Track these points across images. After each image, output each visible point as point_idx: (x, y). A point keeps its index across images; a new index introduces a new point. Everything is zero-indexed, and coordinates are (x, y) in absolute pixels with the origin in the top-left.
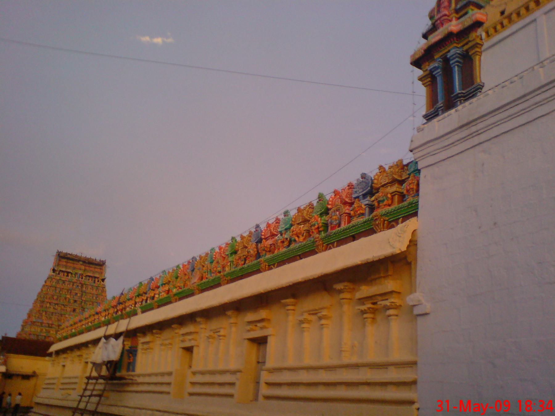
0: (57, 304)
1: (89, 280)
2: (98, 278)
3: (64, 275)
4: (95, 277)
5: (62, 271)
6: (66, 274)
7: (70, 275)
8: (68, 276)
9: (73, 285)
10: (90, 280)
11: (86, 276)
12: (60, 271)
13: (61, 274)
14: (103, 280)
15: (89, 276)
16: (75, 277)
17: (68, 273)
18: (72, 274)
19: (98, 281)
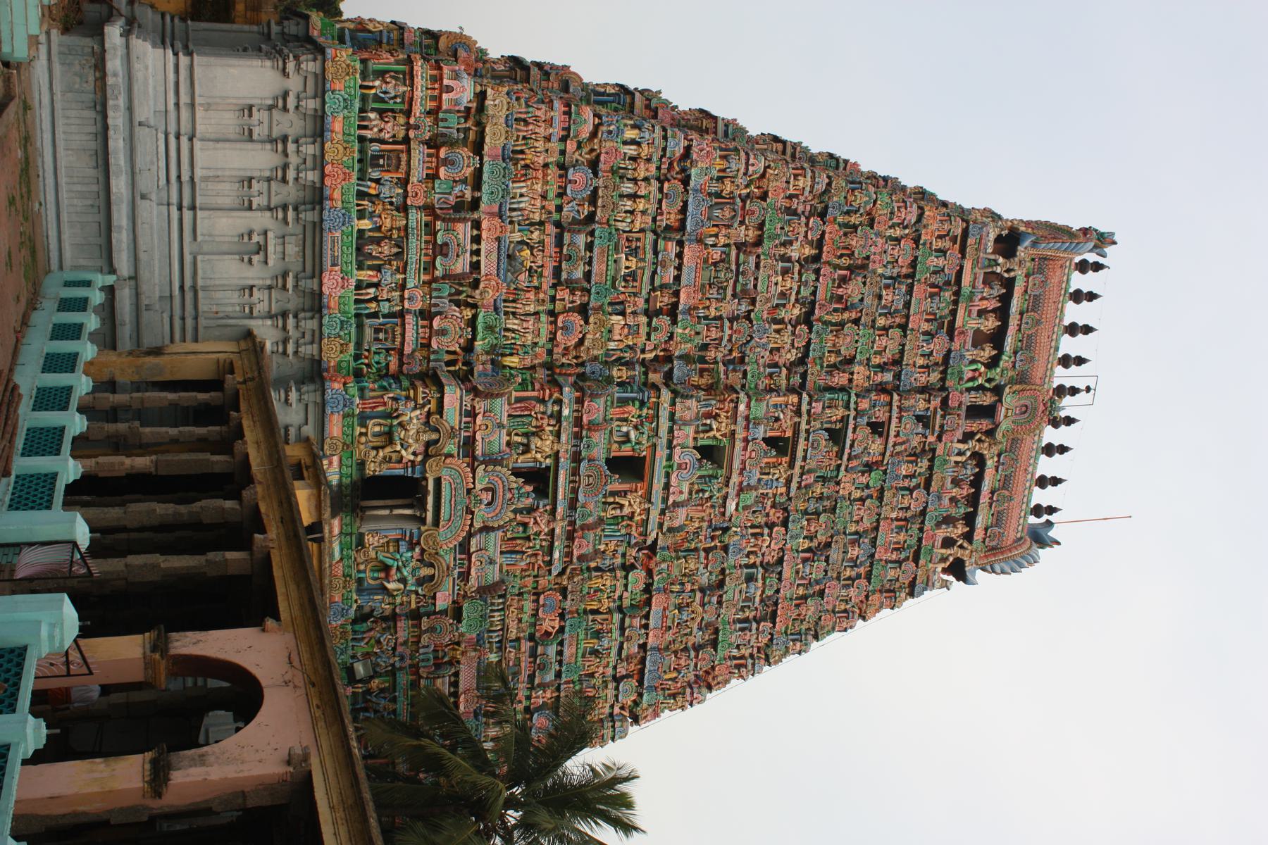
0: (807, 319)
1: (956, 482)
2: (969, 537)
3: (981, 313)
4: (970, 519)
5: (1006, 299)
6: (991, 324)
7: (988, 352)
8: (979, 339)
9: (924, 390)
10: (956, 492)
11: (979, 459)
12: (1009, 284)
13: (989, 297)
14: (958, 570)
15: (977, 482)
16: (969, 390)
17: (997, 338)
18: (993, 363)
19: (948, 543)
